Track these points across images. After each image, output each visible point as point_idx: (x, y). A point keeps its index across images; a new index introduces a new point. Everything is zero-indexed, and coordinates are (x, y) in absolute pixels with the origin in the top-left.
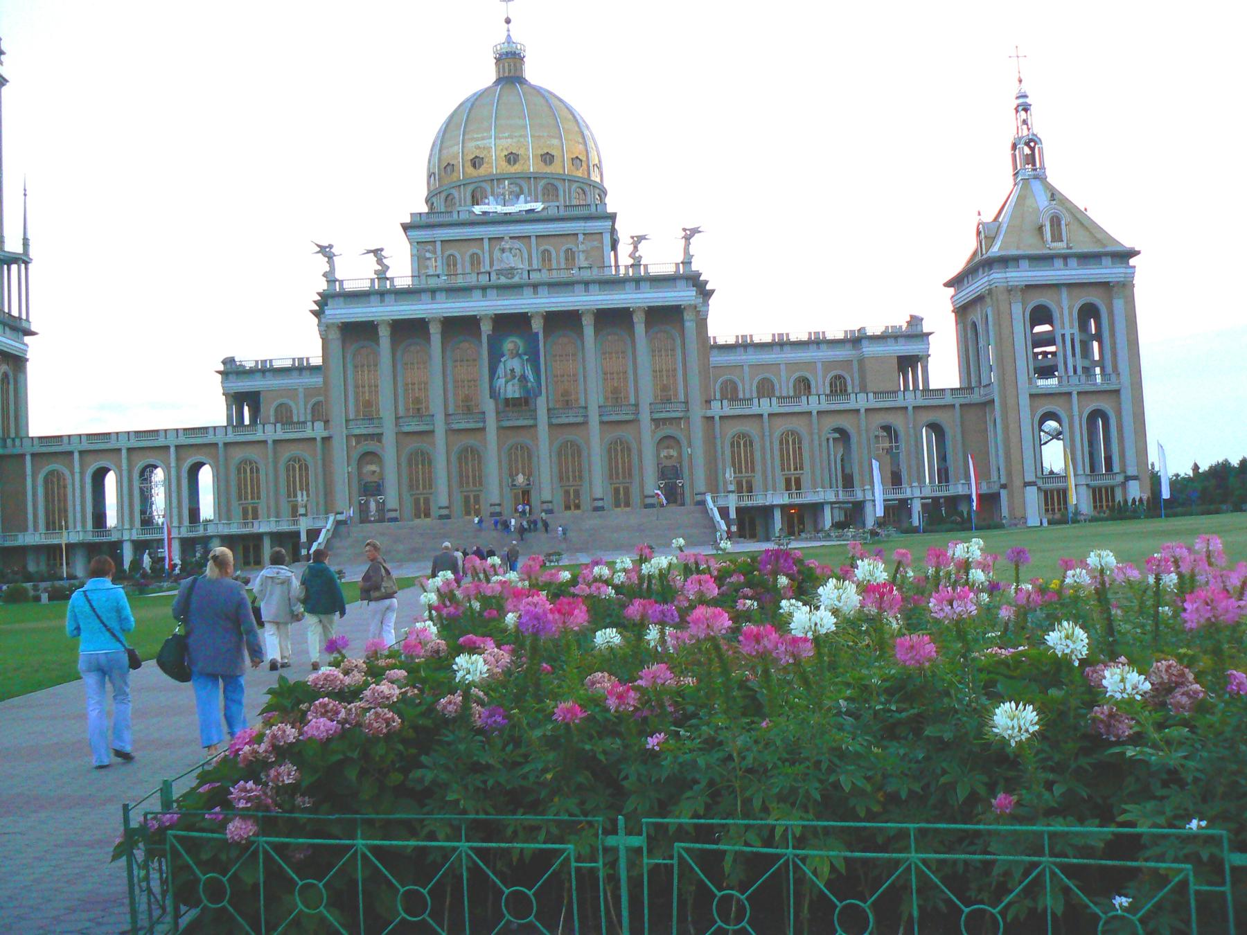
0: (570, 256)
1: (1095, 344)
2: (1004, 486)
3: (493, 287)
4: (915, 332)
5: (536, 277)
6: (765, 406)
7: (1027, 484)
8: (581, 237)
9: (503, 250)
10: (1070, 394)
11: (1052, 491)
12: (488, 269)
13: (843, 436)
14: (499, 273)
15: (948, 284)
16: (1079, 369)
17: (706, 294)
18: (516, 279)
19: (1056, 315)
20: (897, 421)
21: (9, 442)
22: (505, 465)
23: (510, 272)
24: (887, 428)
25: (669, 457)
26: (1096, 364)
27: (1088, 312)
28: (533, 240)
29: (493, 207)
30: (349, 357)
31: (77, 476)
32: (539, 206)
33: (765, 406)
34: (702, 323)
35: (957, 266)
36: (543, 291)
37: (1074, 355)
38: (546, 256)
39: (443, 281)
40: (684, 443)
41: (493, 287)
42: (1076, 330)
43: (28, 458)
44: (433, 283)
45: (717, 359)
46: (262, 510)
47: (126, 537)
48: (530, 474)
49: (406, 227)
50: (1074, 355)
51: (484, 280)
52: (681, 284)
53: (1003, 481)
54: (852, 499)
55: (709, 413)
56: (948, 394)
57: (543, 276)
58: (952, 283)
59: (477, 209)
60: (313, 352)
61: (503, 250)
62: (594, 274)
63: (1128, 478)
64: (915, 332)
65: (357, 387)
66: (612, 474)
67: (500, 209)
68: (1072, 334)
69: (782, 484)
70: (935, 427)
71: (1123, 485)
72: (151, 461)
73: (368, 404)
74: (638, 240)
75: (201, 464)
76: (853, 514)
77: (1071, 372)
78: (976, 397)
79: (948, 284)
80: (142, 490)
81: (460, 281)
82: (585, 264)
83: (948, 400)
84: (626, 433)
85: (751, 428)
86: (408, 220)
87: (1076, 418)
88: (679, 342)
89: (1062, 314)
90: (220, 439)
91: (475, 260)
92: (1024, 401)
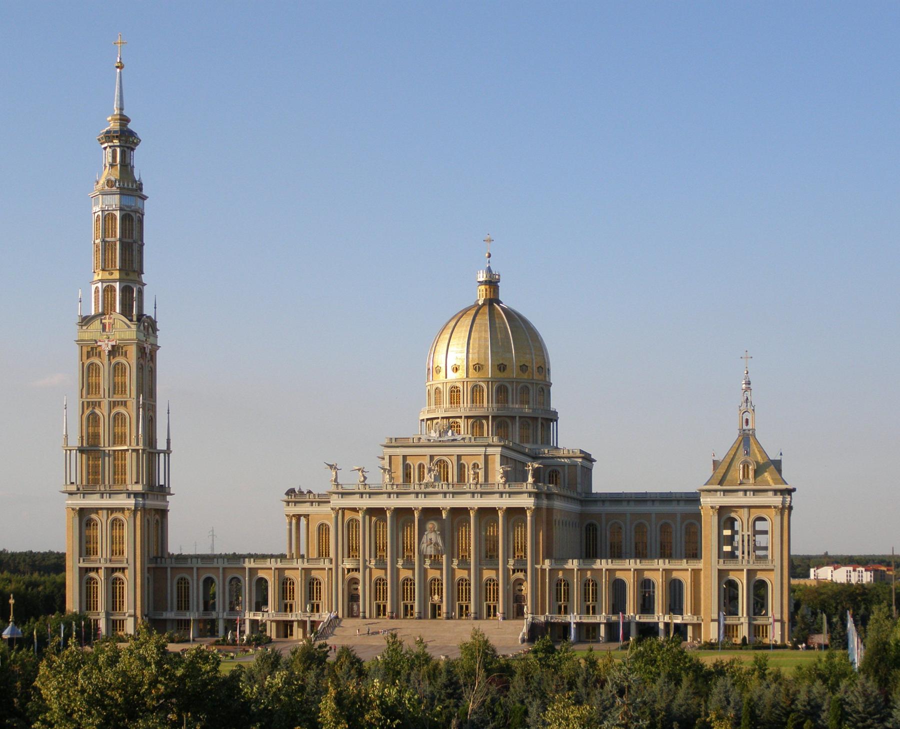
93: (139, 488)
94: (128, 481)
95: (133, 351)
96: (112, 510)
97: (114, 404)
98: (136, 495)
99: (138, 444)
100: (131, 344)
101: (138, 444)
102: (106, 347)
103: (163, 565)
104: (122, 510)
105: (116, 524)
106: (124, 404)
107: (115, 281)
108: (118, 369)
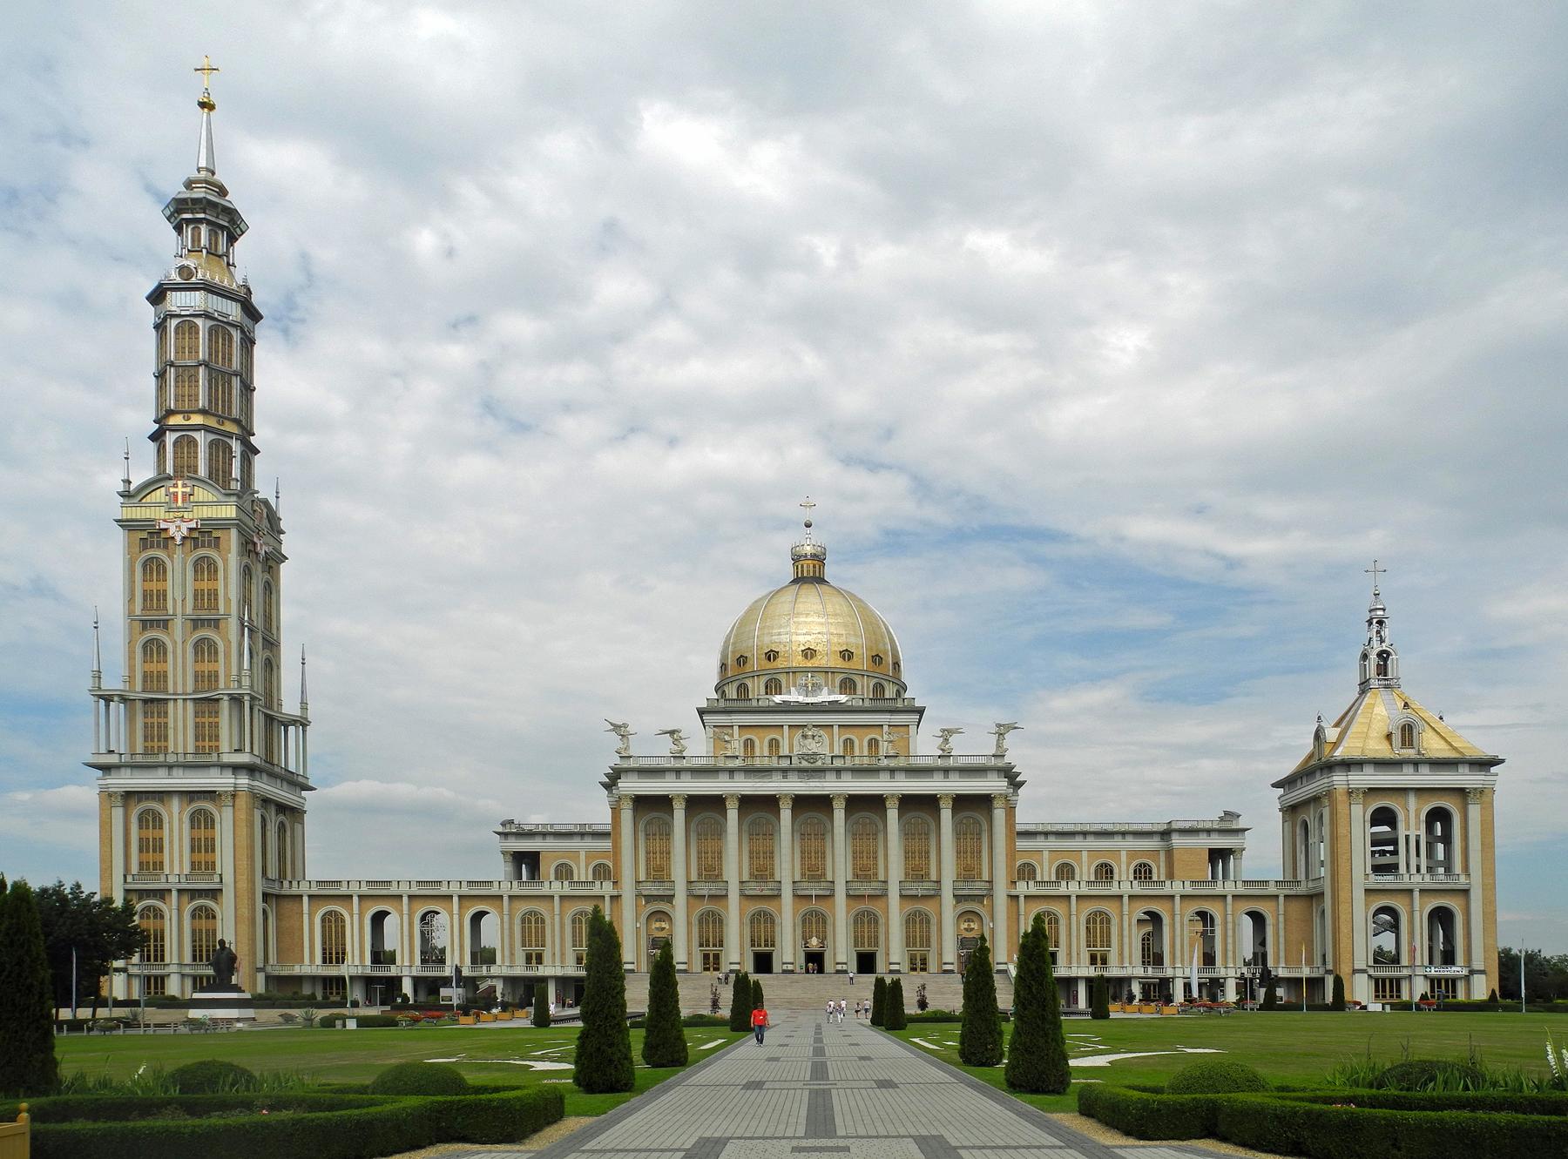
0: (874, 743)
1: (1440, 847)
2: (1328, 972)
3: (793, 770)
4: (1229, 825)
5: (838, 763)
6: (1073, 888)
7: (1355, 971)
8: (886, 728)
9: (805, 737)
10: (1411, 891)
11: (1384, 980)
12: (787, 753)
13: (1155, 918)
14: (802, 757)
15: (1276, 785)
16: (1423, 869)
17: (1015, 782)
18: (819, 763)
19: (1401, 817)
20: (1213, 908)
21: (286, 884)
22: (799, 931)
23: (813, 756)
24: (1203, 915)
25: (969, 930)
26: (1440, 864)
27: (1439, 816)
28: (836, 729)
29: (795, 697)
30: (641, 826)
31: (356, 917)
32: (843, 698)
33: (1073, 888)
34: (1011, 811)
35: (1289, 767)
36: (846, 776)
37: (1418, 855)
38: (848, 743)
39: (738, 763)
40: (986, 919)
41: (793, 770)
42: (1422, 832)
43: (305, 899)
44: (731, 764)
45: (1022, 844)
46: (547, 958)
47: (406, 972)
48: (824, 938)
49: (701, 712)
50: (1418, 855)
51: (785, 763)
52: (993, 776)
53: (1330, 967)
54: (1161, 975)
55: (1014, 893)
56: (1272, 884)
57: (849, 764)
58: (1286, 783)
59: (778, 699)
60: (598, 812)
61: (805, 737)
62: (902, 762)
63: (1472, 972)
64: (1229, 825)
65: (648, 853)
66: (909, 941)
67: (801, 699)
68: (1418, 836)
69: (1086, 958)
70: (1258, 919)
71: (1467, 978)
72: (433, 908)
73: (660, 869)
74: (947, 734)
75: (484, 913)
76: (1158, 991)
77: (1413, 870)
78: (1302, 889)
79: (1276, 785)
80: (422, 933)
81: (758, 763)
82: (892, 753)
83: (1272, 890)
84: (927, 907)
85: (1058, 908)
86: (704, 705)
87: (1417, 915)
88: (985, 827)
89: (1407, 817)
90: (505, 889)
91: (774, 744)
92: (1359, 895)
93: (244, 758)
94: (224, 746)
95: (233, 539)
96: (191, 795)
97: (197, 623)
98: (236, 768)
99: (240, 687)
100: (226, 528)
101: (240, 687)
102: (178, 531)
103: (294, 890)
104: (211, 795)
105: (201, 820)
106: (215, 623)
107: (197, 428)
108: (204, 568)
